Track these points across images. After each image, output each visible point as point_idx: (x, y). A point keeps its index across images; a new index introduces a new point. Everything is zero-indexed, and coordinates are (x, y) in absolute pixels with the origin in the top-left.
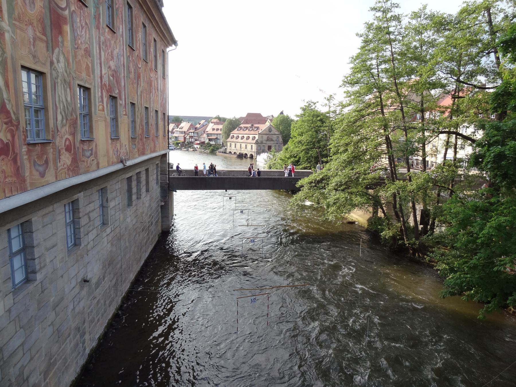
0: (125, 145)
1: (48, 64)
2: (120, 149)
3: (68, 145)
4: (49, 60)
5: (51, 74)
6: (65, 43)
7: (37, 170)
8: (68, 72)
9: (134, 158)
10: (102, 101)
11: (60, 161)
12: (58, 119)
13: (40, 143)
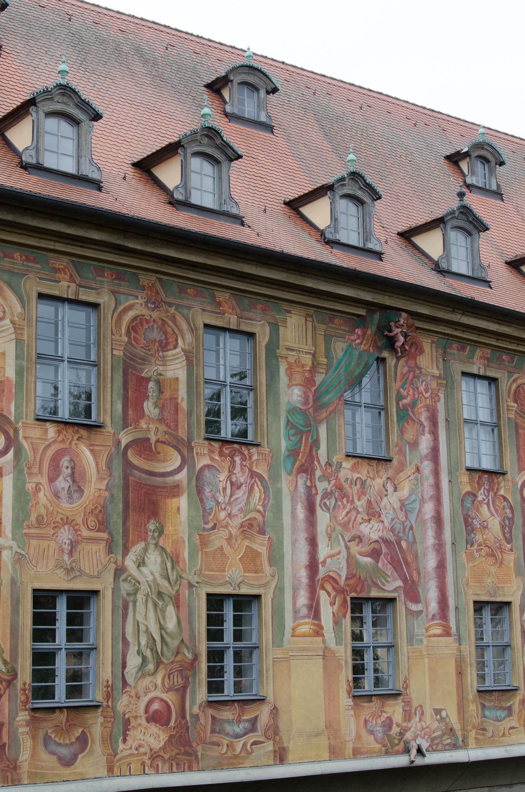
1: (109, 576)
3: (156, 712)
4: (113, 567)
5: (115, 591)
6: (169, 529)
7: (53, 753)
8: (173, 577)
11: (125, 741)
13: (67, 708)
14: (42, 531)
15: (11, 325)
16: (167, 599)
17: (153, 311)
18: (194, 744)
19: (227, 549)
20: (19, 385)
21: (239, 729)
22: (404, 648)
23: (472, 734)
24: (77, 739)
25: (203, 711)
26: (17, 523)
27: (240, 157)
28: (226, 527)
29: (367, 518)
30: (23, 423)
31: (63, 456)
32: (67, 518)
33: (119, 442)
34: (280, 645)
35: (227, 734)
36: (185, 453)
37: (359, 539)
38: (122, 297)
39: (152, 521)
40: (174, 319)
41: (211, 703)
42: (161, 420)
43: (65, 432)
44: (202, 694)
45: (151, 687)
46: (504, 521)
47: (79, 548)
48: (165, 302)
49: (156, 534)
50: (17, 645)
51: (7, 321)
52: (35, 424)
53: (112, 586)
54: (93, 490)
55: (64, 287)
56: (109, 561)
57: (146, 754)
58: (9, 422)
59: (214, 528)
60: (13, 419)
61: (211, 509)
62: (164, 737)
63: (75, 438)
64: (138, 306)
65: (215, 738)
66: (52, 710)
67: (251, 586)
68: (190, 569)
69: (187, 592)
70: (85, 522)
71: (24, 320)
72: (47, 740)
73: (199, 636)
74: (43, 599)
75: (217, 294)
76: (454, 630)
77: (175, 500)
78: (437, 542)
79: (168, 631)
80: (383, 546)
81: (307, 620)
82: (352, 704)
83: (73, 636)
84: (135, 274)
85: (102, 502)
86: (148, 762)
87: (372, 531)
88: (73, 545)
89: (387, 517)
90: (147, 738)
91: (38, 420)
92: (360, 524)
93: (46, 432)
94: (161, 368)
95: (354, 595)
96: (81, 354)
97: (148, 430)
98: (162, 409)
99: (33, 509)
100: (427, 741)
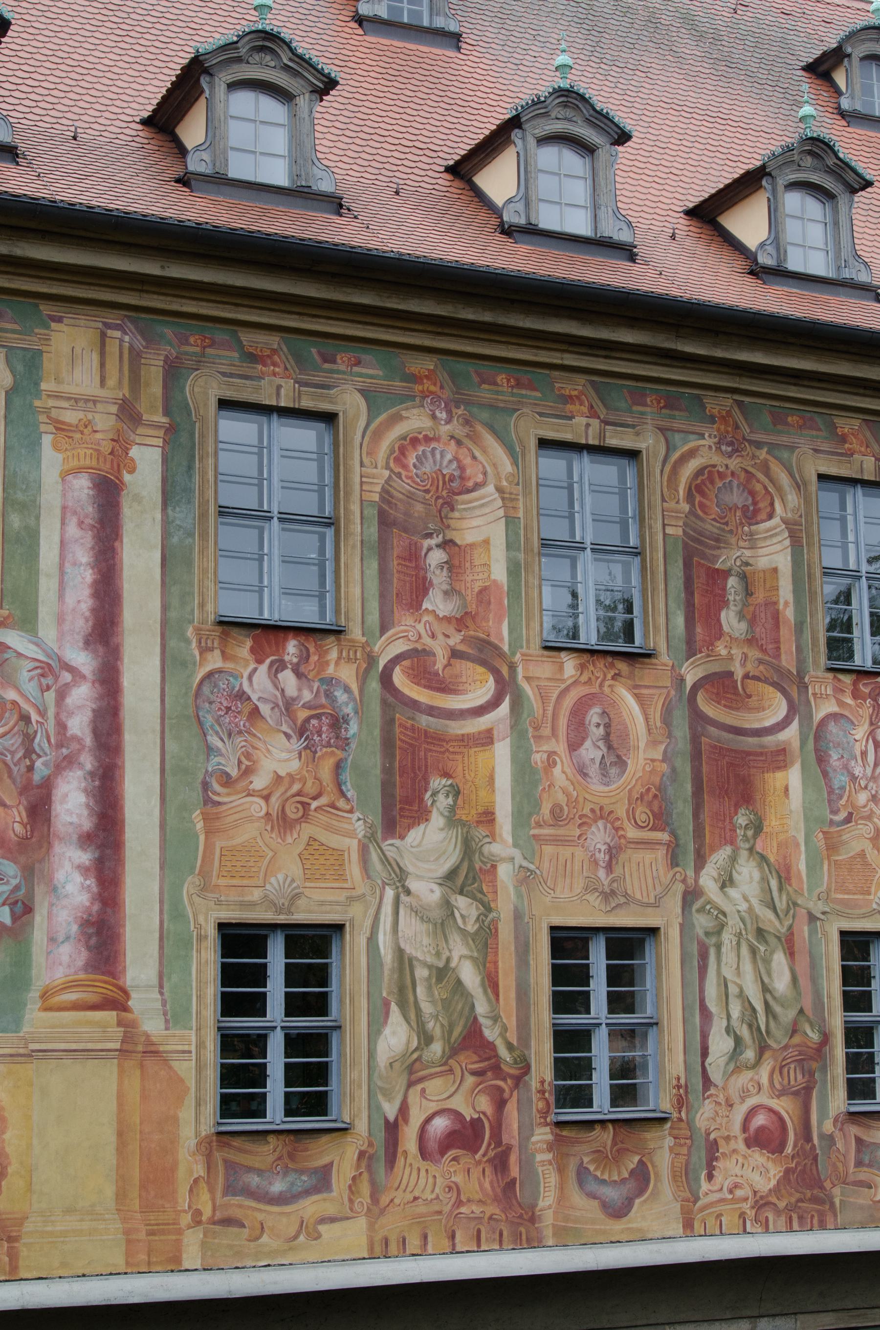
1: (674, 904)
3: (761, 1129)
4: (679, 888)
5: (685, 928)
6: (772, 823)
7: (592, 1196)
8: (781, 905)
11: (710, 1177)
12: (712, 1048)
14: (561, 832)
15: (497, 495)
16: (773, 941)
17: (730, 457)
18: (827, 1185)
20: (514, 592)
24: (632, 1173)
25: (841, 1130)
26: (521, 818)
27: (869, 184)
28: (869, 818)
30: (522, 655)
31: (590, 706)
32: (601, 808)
33: (682, 680)
36: (795, 695)
38: (677, 437)
39: (742, 811)
40: (765, 468)
41: (853, 1116)
42: (751, 641)
43: (591, 668)
44: (838, 1100)
45: (751, 1089)
47: (623, 857)
48: (751, 442)
49: (750, 833)
50: (528, 1018)
51: (490, 489)
52: (542, 656)
53: (680, 920)
54: (641, 762)
55: (581, 427)
56: (673, 879)
57: (746, 1199)
58: (501, 655)
59: (848, 820)
60: (506, 648)
61: (843, 788)
62: (775, 1172)
63: (609, 676)
64: (704, 451)
65: (864, 1175)
66: (589, 1124)
68: (810, 890)
69: (806, 928)
70: (631, 815)
71: (518, 484)
72: (582, 1173)
73: (829, 1002)
74: (568, 943)
75: (839, 422)
77: (779, 775)
79: (777, 995)
83: (620, 1002)
84: (698, 398)
85: (657, 780)
86: (750, 1213)
88: (613, 853)
90: (747, 1172)
91: (546, 648)
93: (561, 668)
94: (747, 553)
96: (612, 537)
97: (730, 658)
98: (752, 622)
99: (545, 795)
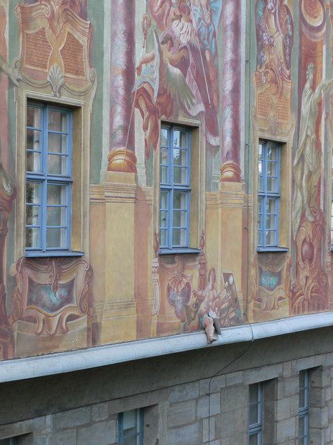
0: (227, 276)
2: (202, 286)
9: (264, 315)
10: (130, 141)
18: (10, 321)
19: (48, 33)
21: (54, 298)
22: (203, 195)
23: (251, 305)
25: (21, 272)
29: (178, 14)
34: (97, 182)
35: (44, 306)
37: (169, 40)
46: (286, 39)
65: (32, 313)
67: (72, 92)
69: (7, 92)
73: (18, 160)
76: (242, 174)
78: (234, 57)
80: (190, 53)
81: (122, 148)
82: (157, 265)
87: (182, 31)
89: (196, 13)
92: (173, 20)
95: (164, 118)
100: (217, 314)
